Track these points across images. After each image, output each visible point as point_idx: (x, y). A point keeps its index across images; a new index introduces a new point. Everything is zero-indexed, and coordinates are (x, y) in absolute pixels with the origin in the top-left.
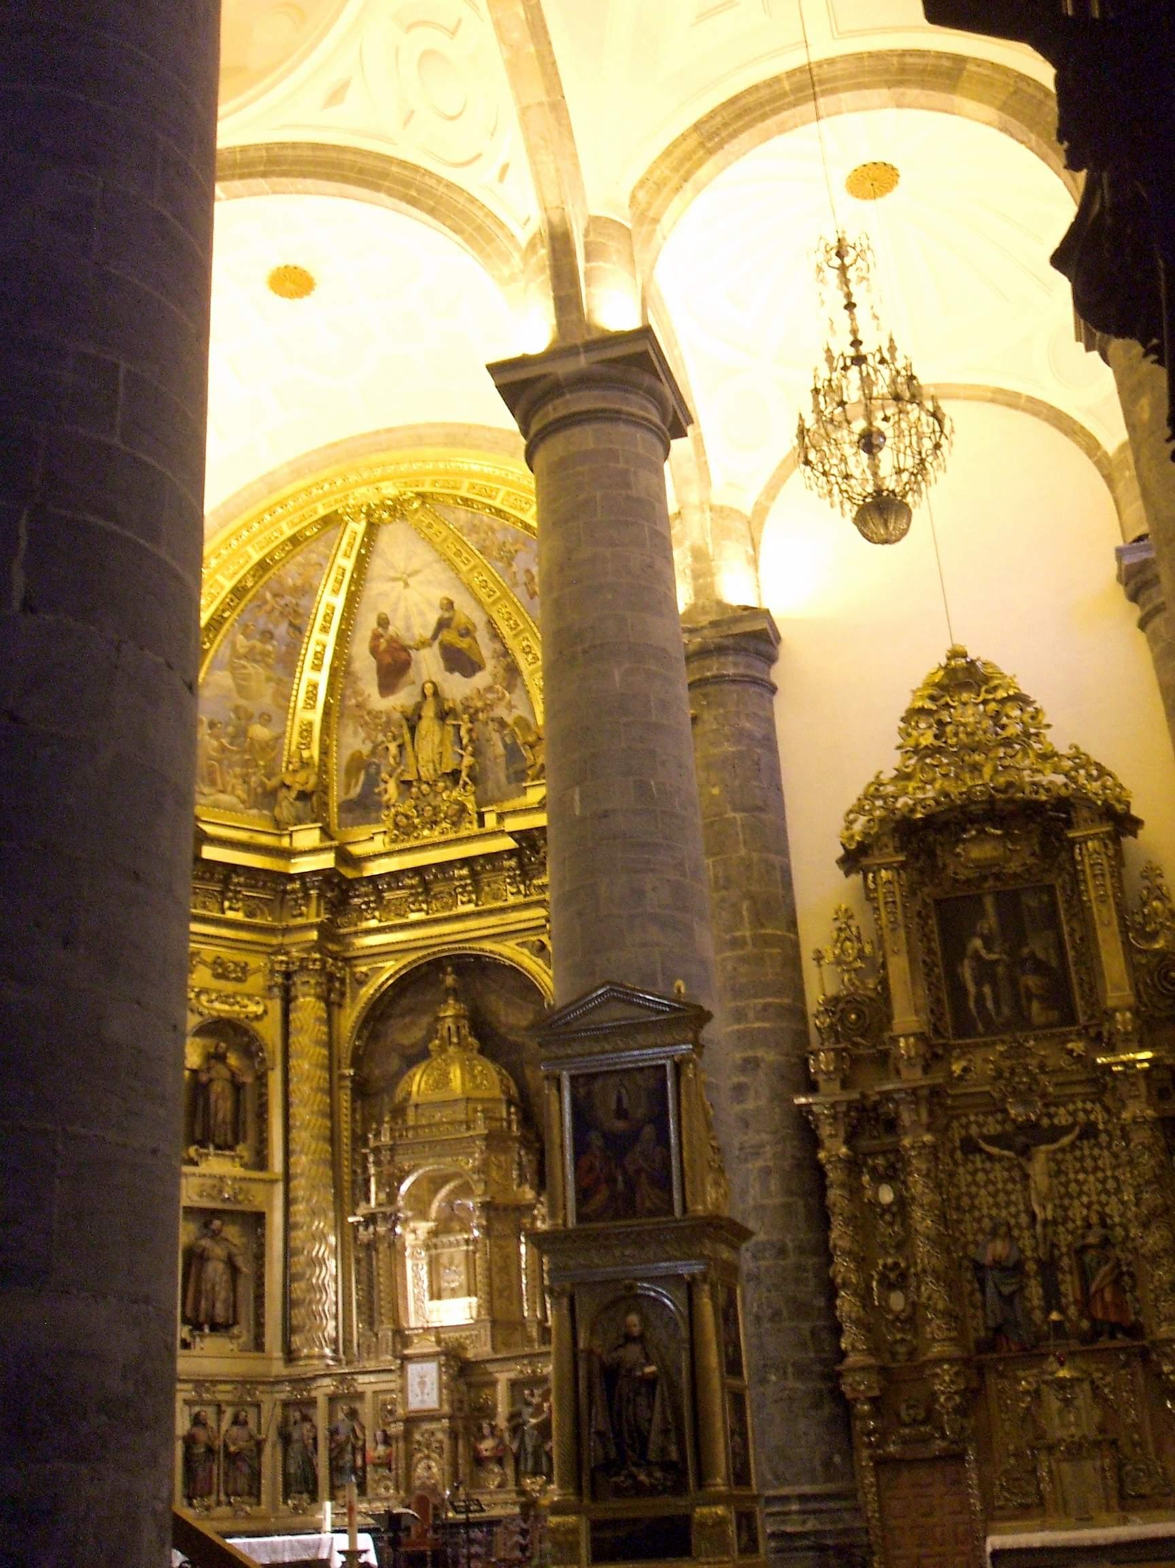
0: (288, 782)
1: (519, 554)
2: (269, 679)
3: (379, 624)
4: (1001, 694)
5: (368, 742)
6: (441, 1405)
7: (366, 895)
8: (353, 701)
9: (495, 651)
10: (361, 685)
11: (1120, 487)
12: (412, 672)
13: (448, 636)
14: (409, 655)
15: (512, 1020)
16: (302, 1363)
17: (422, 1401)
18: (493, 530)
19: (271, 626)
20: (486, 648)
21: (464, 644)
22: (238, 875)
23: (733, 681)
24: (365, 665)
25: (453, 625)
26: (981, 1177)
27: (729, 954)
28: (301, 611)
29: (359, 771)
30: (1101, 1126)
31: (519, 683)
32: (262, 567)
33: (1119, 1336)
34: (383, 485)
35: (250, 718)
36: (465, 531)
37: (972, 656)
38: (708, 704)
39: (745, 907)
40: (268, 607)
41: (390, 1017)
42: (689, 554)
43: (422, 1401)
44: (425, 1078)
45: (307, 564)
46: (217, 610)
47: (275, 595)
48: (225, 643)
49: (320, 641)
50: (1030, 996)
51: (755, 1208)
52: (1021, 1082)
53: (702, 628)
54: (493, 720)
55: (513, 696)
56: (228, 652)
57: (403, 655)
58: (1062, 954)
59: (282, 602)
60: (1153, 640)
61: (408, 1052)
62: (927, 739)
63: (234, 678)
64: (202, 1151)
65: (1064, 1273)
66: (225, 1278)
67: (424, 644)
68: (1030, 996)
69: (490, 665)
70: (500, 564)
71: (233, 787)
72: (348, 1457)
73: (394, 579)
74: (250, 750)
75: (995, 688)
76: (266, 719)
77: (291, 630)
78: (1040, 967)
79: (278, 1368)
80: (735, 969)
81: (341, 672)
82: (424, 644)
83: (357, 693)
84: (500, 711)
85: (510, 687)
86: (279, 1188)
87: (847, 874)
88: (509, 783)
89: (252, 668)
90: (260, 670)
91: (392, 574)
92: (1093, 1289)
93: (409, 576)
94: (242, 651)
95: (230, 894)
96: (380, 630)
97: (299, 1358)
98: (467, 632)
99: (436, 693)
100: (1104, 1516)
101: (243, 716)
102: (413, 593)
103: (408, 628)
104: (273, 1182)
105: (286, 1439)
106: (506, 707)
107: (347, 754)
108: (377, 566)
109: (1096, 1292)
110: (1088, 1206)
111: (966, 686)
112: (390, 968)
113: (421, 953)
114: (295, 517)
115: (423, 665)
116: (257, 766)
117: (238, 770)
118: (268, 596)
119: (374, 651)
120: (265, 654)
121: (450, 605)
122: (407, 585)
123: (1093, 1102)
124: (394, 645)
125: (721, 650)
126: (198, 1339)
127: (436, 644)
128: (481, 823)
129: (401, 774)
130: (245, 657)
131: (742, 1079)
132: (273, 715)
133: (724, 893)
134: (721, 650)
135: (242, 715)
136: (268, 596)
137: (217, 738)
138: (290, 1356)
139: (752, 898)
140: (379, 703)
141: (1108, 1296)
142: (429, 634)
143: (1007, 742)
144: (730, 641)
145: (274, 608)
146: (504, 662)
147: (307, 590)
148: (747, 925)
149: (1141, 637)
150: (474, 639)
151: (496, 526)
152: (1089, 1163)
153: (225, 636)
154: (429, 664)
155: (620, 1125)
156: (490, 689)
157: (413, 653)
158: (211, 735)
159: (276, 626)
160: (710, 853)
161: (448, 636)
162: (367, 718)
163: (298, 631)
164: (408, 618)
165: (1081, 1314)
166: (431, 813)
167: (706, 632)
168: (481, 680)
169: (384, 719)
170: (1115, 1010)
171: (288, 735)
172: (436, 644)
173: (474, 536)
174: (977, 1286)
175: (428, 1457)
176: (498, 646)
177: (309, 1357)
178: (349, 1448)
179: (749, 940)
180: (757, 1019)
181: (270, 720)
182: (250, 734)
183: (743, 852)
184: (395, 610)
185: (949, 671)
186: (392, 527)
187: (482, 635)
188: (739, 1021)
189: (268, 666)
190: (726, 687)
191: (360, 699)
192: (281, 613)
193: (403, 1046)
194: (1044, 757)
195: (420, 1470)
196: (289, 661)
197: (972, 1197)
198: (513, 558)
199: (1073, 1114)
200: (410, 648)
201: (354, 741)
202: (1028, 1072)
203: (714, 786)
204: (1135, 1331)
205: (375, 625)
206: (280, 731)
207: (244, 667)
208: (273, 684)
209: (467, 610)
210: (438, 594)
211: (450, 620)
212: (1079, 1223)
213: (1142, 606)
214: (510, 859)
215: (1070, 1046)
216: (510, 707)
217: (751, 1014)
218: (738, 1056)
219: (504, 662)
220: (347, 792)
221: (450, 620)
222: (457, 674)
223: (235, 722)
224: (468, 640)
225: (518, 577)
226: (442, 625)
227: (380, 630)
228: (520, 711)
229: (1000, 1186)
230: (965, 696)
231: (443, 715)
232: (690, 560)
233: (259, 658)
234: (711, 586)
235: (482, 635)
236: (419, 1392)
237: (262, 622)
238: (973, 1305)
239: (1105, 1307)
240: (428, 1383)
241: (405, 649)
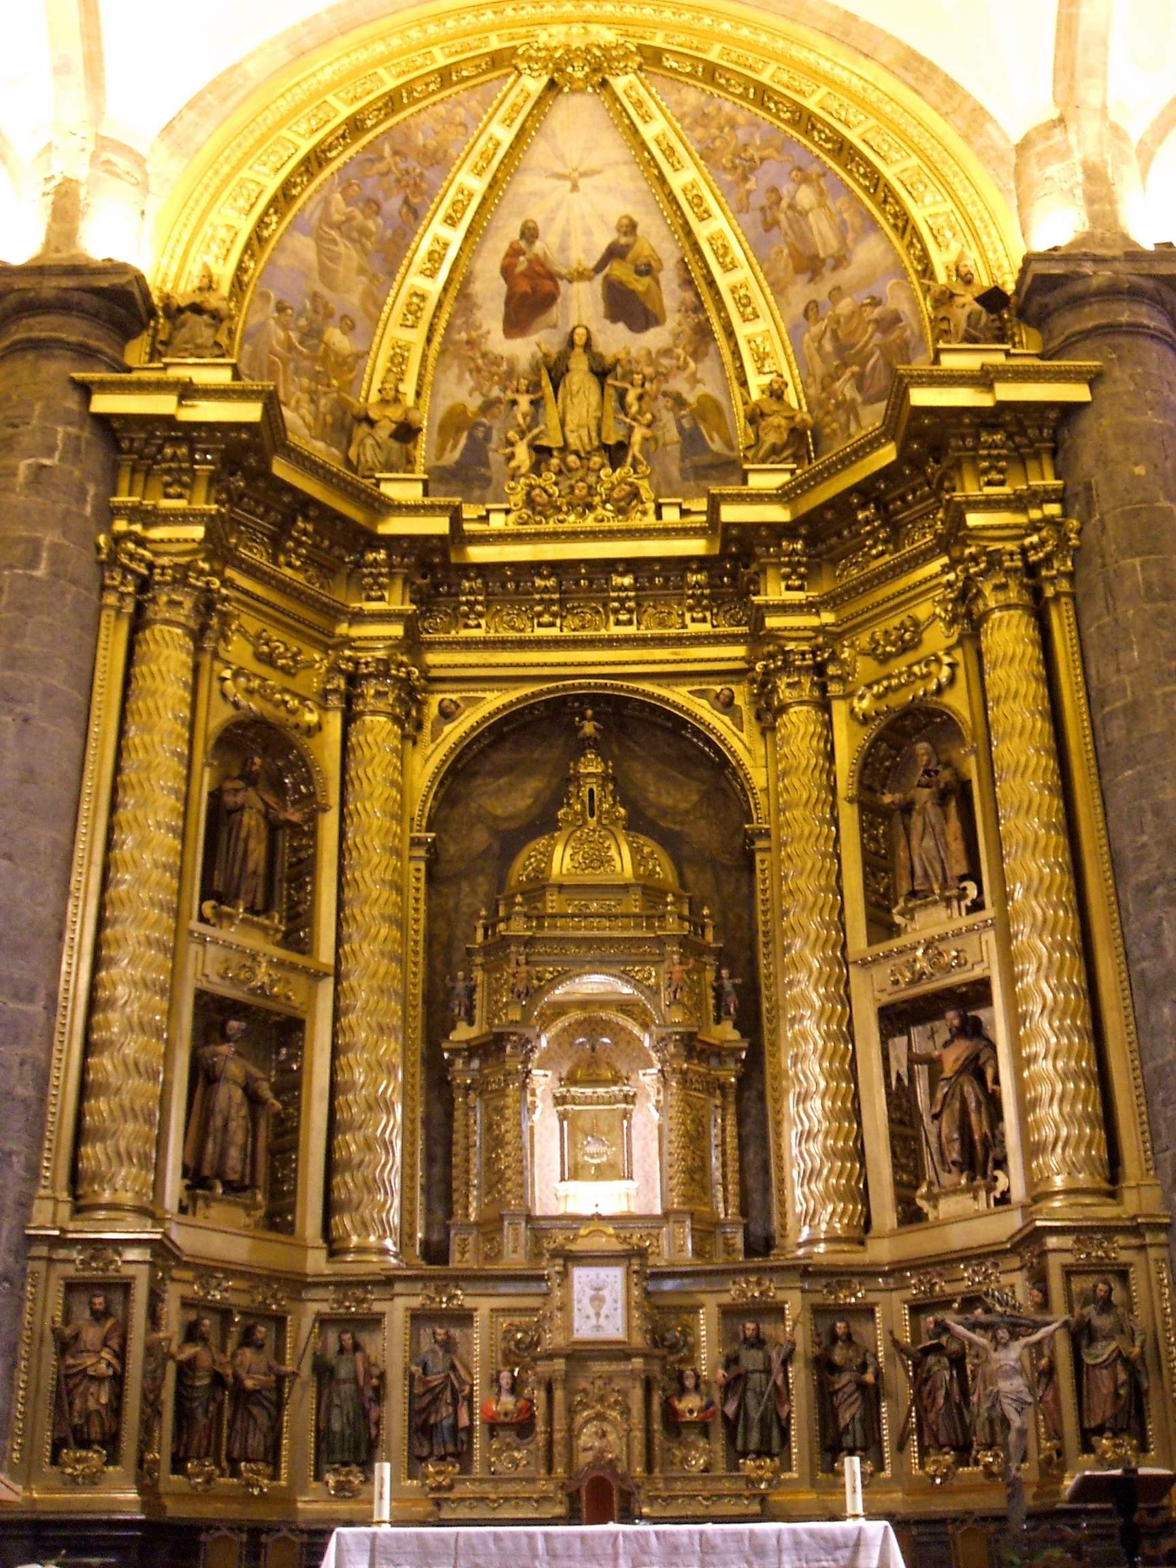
0: (374, 414)
1: (766, 165)
2: (362, 271)
3: (523, 235)
5: (477, 394)
6: (629, 1335)
7: (472, 592)
8: (464, 336)
9: (683, 303)
10: (478, 315)
12: (555, 312)
13: (619, 270)
14: (557, 286)
15: (666, 801)
16: (350, 1258)
17: (598, 1327)
18: (733, 125)
19: (380, 196)
20: (670, 295)
21: (640, 285)
22: (307, 518)
23: (1152, 337)
24: (490, 289)
25: (630, 256)
28: (424, 186)
29: (459, 430)
31: (712, 349)
32: (392, 102)
34: (593, 28)
35: (330, 315)
36: (687, 121)
38: (1120, 358)
40: (382, 167)
41: (475, 774)
42: (1079, 170)
43: (598, 1327)
44: (569, 851)
45: (447, 121)
46: (323, 141)
47: (396, 153)
48: (318, 197)
49: (440, 234)
53: (1114, 259)
54: (665, 394)
55: (701, 366)
56: (318, 214)
57: (547, 286)
59: (403, 166)
61: (505, 826)
63: (319, 253)
64: (226, 909)
66: (243, 1112)
67: (582, 275)
69: (673, 320)
70: (729, 178)
71: (298, 402)
72: (446, 1411)
73: (560, 177)
74: (324, 359)
76: (348, 325)
77: (404, 210)
79: (316, 1262)
81: (460, 290)
82: (582, 275)
83: (469, 326)
84: (678, 384)
85: (696, 355)
86: (326, 989)
88: (685, 479)
89: (344, 248)
90: (354, 253)
91: (559, 168)
93: (584, 175)
94: (337, 217)
95: (291, 544)
96: (523, 244)
97: (347, 1251)
98: (647, 270)
99: (588, 345)
101: (322, 312)
102: (580, 203)
103: (563, 249)
104: (317, 976)
105: (324, 1372)
106: (688, 380)
107: (444, 405)
108: (539, 152)
112: (494, 700)
113: (544, 687)
114: (457, 44)
115: (574, 304)
116: (329, 385)
117: (305, 382)
118: (387, 151)
119: (507, 272)
120: (364, 232)
122: (575, 188)
124: (538, 268)
125: (1134, 294)
126: (200, 1203)
127: (599, 278)
128: (659, 516)
129: (536, 437)
130: (338, 227)
132: (358, 322)
133: (1162, 605)
134: (1134, 294)
135: (321, 311)
136: (387, 151)
137: (285, 328)
138: (334, 1249)
140: (498, 343)
142: (592, 264)
144: (1149, 284)
145: (388, 172)
146: (693, 319)
147: (439, 160)
150: (657, 282)
151: (741, 118)
153: (316, 191)
154: (582, 305)
156: (667, 352)
157: (563, 285)
158: (278, 321)
159: (388, 196)
160: (1132, 550)
161: (619, 270)
162: (480, 362)
163: (415, 214)
164: (566, 234)
166: (584, 492)
167: (1118, 266)
168: (655, 338)
169: (504, 367)
171: (372, 354)
172: (599, 278)
173: (699, 132)
175: (600, 1417)
176: (689, 296)
177: (361, 1250)
178: (448, 1395)
181: (352, 328)
182: (326, 337)
184: (552, 220)
186: (576, 100)
187: (669, 279)
189: (364, 251)
190: (1147, 343)
191: (474, 334)
192: (398, 181)
193: (495, 818)
195: (587, 1437)
196: (390, 256)
198: (752, 170)
200: (562, 277)
201: (460, 392)
203: (1136, 464)
205: (516, 235)
206: (362, 348)
207: (335, 242)
208: (363, 278)
209: (656, 239)
210: (617, 209)
211: (628, 247)
214: (698, 571)
216: (694, 380)
219: (693, 319)
220: (439, 458)
221: (628, 247)
222: (621, 326)
223: (310, 314)
224: (647, 280)
225: (752, 199)
226: (614, 253)
227: (523, 244)
228: (708, 388)
231: (602, 372)
232: (1080, 177)
233: (355, 235)
234: (1114, 214)
235: (669, 279)
236: (591, 1312)
237: (371, 187)
240: (609, 1300)
241: (552, 277)
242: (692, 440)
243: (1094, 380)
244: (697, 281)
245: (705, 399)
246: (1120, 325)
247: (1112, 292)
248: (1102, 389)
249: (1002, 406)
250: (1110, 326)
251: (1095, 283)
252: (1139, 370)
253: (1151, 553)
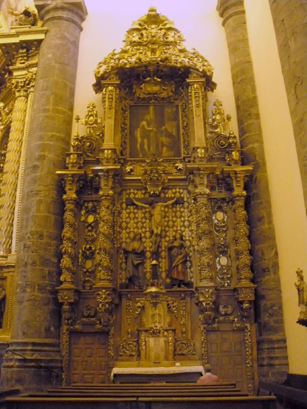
4: (168, 26)
23: (66, 20)
26: (132, 215)
27: (42, 114)
30: (185, 200)
33: (182, 286)
37: (158, 12)
39: (51, 98)
50: (163, 145)
51: (33, 216)
52: (154, 176)
58: (178, 131)
62: (136, 39)
65: (162, 258)
68: (163, 145)
75: (166, 24)
78: (169, 135)
80: (43, 120)
87: (96, 93)
92: (173, 265)
100: (166, 362)
109: (175, 266)
110: (176, 231)
111: (155, 23)
123: (184, 189)
125: (62, 8)
131: (37, 163)
134: (62, 8)
139: (56, 95)
141: (180, 267)
143: (167, 44)
144: (66, 6)
148: (51, 104)
149: (223, 29)
152: (178, 214)
165: (167, 276)
170: (198, 148)
174: (124, 260)
179: (51, 110)
180: (48, 140)
183: (55, 78)
185: (149, 16)
188: (40, 140)
194: (181, 51)
197: (127, 223)
199: (175, 193)
202: (157, 172)
204: (189, 285)
212: (171, 238)
215: (176, 165)
217: (46, 138)
218: (37, 154)
229: (140, 220)
230: (153, 26)
238: (121, 269)
239: (178, 273)
243: (46, 32)
246: (55, 17)
247: (56, 9)
248: (48, 35)
249: (22, 42)
250: (52, 18)
251: (51, 6)
252: (58, 29)
253: (46, 78)
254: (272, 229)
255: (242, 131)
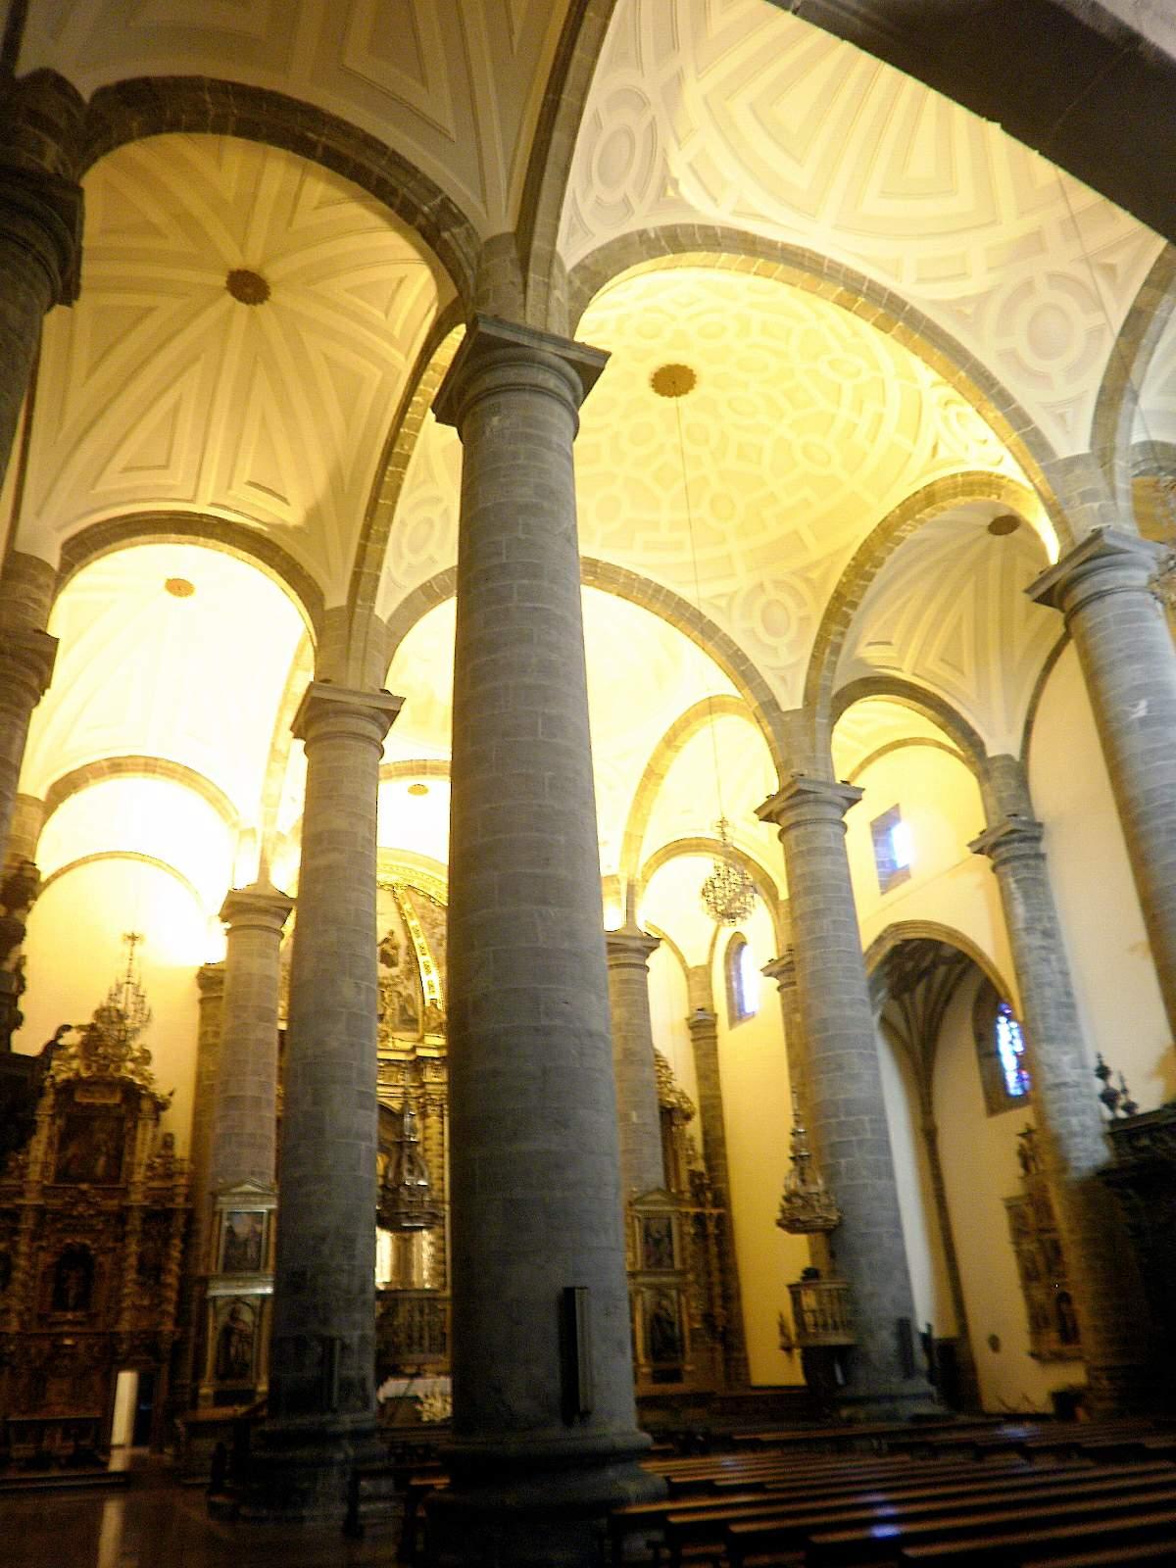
11: (692, 982)
13: (386, 946)
21: (392, 952)
60: (697, 1048)
84: (400, 988)
85: (408, 979)
98: (395, 948)
121: (392, 933)
149: (691, 1044)
155: (657, 1236)
156: (398, 977)
161: (386, 946)
168: (395, 971)
194: (671, 1091)
209: (400, 939)
213: (694, 1033)
216: (405, 988)
226: (386, 941)
242: (403, 1009)
244: (413, 960)
245: (410, 995)
254: (736, 1264)
255: (710, 1168)
